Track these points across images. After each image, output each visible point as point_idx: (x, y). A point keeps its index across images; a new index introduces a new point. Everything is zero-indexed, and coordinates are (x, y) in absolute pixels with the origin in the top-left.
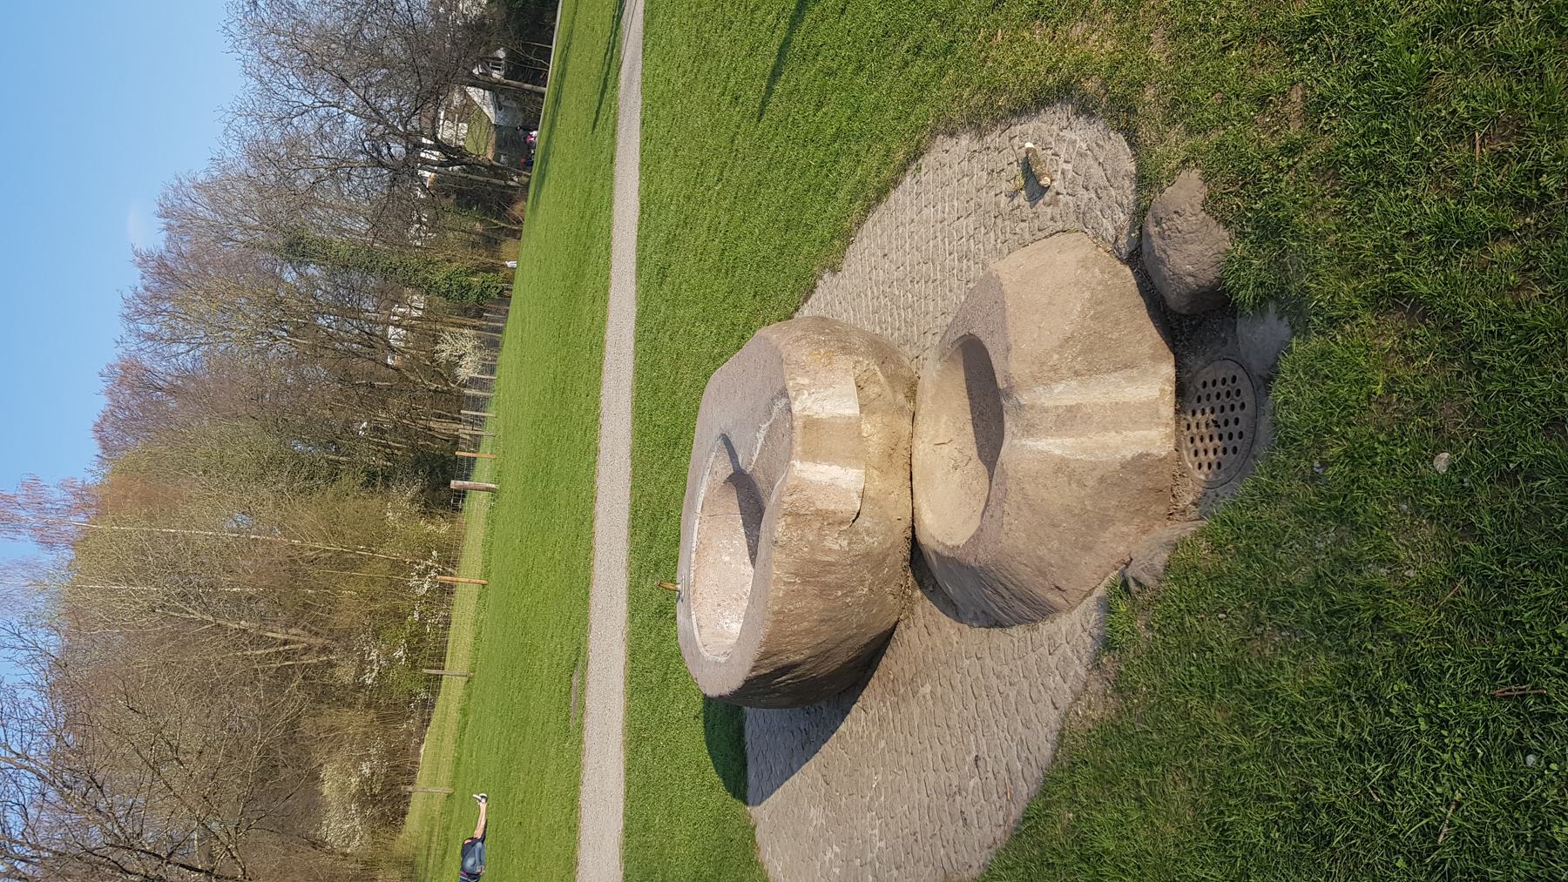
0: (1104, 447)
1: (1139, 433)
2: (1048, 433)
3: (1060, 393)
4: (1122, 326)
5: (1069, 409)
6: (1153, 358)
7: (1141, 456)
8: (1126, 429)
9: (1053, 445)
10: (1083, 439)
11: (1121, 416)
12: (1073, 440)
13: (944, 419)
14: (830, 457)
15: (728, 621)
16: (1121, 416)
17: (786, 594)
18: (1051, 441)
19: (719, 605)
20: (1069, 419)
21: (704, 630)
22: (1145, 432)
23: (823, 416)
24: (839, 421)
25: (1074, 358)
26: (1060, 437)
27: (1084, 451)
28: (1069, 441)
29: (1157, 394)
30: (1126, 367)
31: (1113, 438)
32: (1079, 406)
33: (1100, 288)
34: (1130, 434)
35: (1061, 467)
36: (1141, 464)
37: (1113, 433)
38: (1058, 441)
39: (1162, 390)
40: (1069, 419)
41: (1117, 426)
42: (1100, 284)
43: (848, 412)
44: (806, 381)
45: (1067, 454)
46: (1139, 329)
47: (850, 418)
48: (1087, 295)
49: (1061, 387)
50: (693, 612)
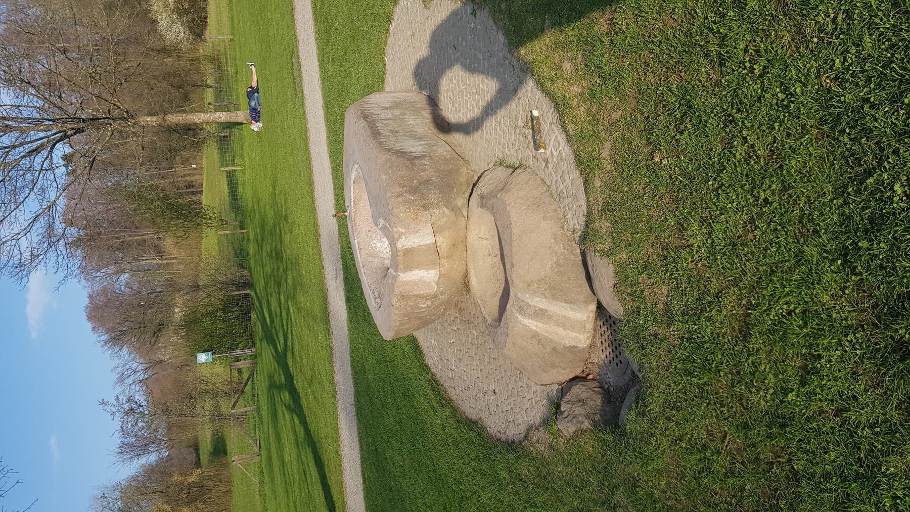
0: (556, 334)
1: (575, 334)
2: (530, 317)
3: (537, 301)
4: (571, 282)
5: (542, 310)
6: (585, 302)
7: (574, 347)
8: (569, 329)
9: (532, 324)
10: (547, 326)
11: (564, 323)
12: (541, 324)
13: (483, 228)
14: (420, 266)
15: (375, 242)
16: (564, 323)
17: (400, 324)
18: (531, 321)
19: (369, 231)
20: (540, 314)
21: (363, 251)
22: (578, 335)
23: (415, 246)
24: (423, 247)
25: (545, 290)
26: (536, 321)
27: (547, 332)
28: (540, 325)
29: (586, 318)
30: (571, 302)
31: (561, 331)
32: (546, 310)
33: (562, 257)
34: (570, 333)
35: (535, 335)
36: (572, 349)
37: (561, 329)
38: (535, 323)
39: (588, 317)
40: (540, 314)
41: (564, 326)
42: (562, 255)
43: (428, 242)
44: (403, 230)
45: (538, 330)
46: (580, 286)
47: (429, 244)
48: (555, 259)
49: (538, 299)
50: (355, 238)
